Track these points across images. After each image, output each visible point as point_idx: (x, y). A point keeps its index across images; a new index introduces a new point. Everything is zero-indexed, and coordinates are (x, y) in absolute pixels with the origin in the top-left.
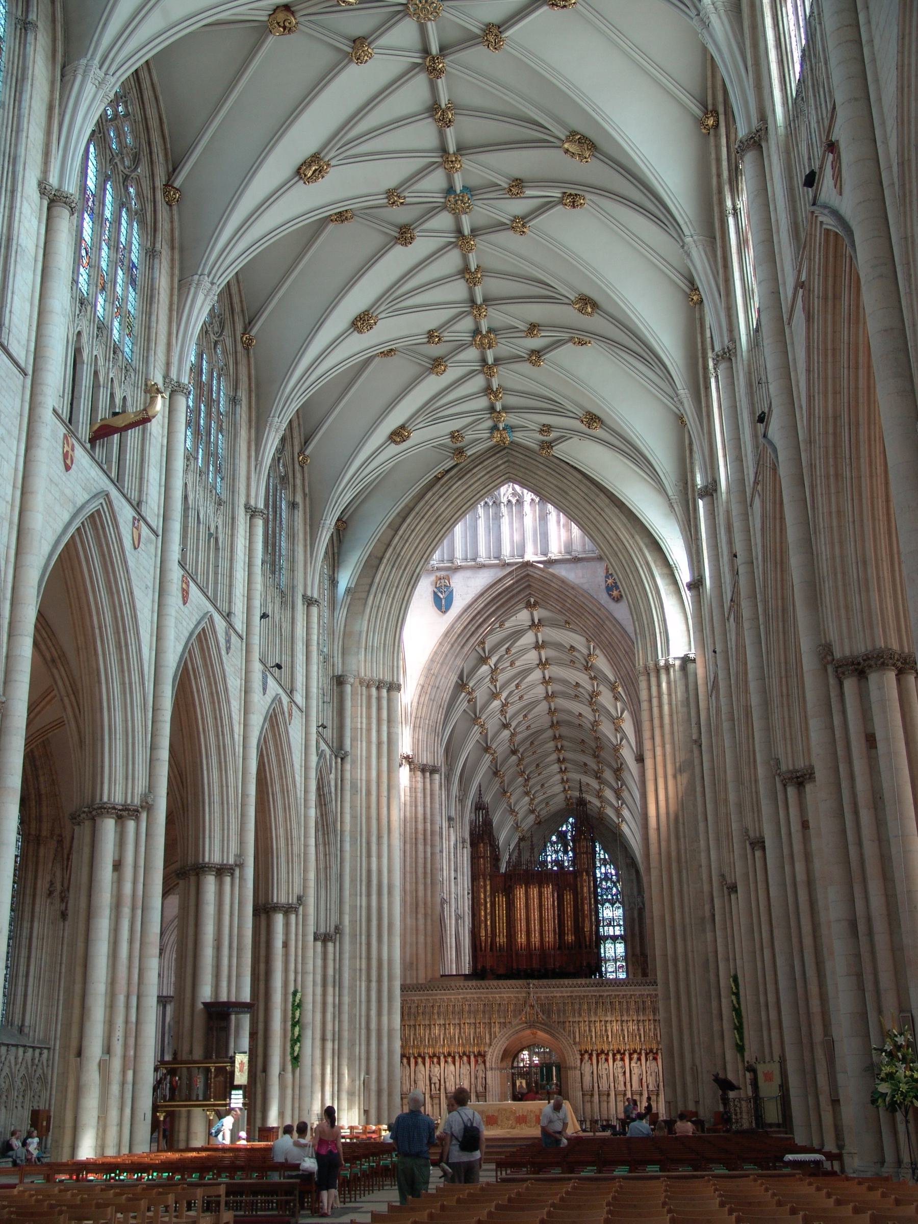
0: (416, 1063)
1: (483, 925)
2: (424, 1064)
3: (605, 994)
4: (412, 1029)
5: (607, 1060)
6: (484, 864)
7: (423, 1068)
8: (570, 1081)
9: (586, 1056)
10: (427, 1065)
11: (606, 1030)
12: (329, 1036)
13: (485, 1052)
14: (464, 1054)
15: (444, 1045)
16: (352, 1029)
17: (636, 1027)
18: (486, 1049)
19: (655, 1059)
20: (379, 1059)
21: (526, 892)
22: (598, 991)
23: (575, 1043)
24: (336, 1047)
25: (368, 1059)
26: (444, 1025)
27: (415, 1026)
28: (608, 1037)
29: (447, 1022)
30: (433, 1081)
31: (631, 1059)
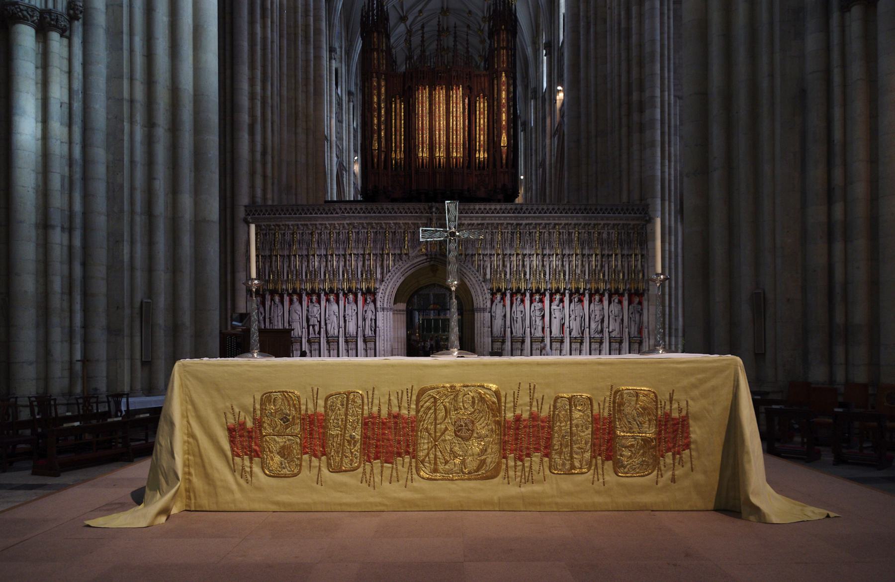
0: (291, 302)
1: (376, 136)
2: (301, 303)
3: (524, 222)
4: (286, 260)
5: (523, 301)
6: (378, 59)
7: (299, 308)
8: (477, 325)
9: (499, 296)
10: (305, 303)
11: (523, 266)
12: (57, 218)
13: (376, 289)
14: (350, 290)
15: (325, 280)
16: (114, 214)
17: (560, 263)
18: (377, 286)
19: (581, 301)
20: (175, 268)
21: (431, 94)
22: (516, 218)
23: (485, 281)
24: (77, 242)
25: (150, 270)
26: (326, 256)
27: (289, 256)
28: (525, 274)
29: (330, 252)
30: (311, 323)
31: (551, 301)
